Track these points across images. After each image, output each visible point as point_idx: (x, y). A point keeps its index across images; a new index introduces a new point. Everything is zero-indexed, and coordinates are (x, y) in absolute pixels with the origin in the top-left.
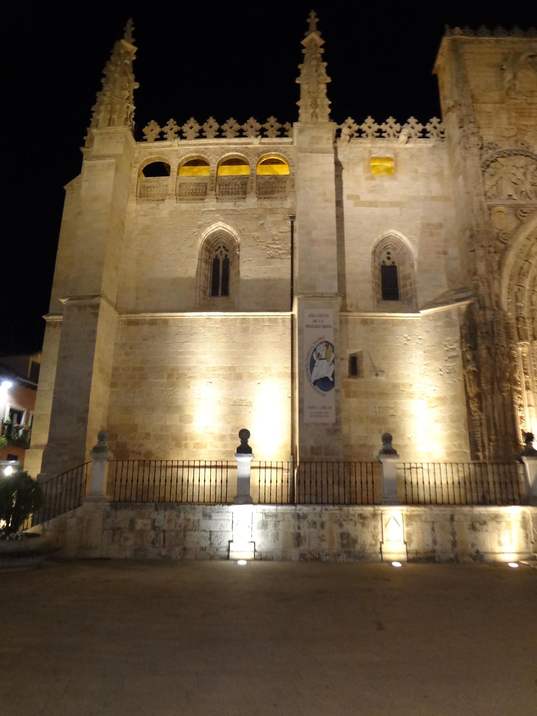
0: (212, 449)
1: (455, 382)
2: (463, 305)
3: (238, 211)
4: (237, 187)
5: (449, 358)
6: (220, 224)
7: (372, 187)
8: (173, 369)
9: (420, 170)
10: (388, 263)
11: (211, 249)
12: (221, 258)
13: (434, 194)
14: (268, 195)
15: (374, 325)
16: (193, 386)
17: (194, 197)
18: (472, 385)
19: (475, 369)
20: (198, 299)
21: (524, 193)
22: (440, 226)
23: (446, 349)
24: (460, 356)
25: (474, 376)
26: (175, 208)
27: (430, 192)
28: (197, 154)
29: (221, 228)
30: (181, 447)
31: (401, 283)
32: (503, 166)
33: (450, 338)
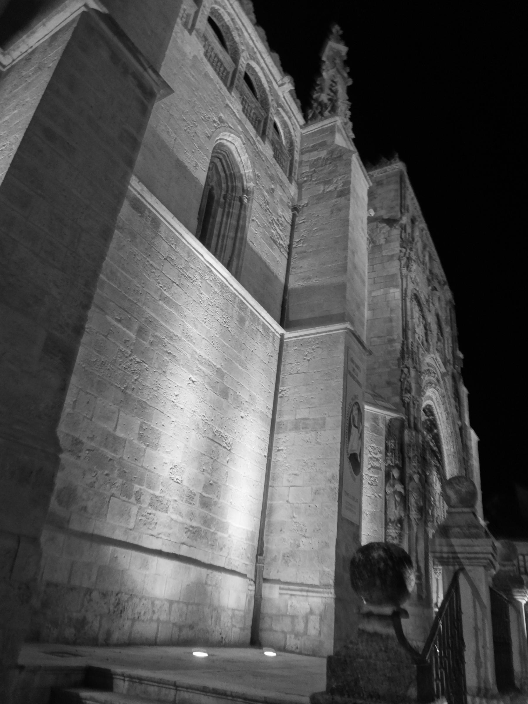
0: (175, 517)
1: (376, 497)
2: (390, 415)
3: (257, 147)
5: (372, 467)
6: (238, 143)
8: (150, 321)
16: (172, 374)
18: (398, 508)
23: (370, 456)
24: (383, 469)
25: (401, 499)
28: (230, 23)
29: (232, 148)
30: (129, 496)
33: (374, 445)
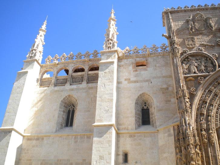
4: (79, 79)
7: (136, 74)
9: (157, 65)
10: (145, 108)
11: (67, 106)
12: (71, 110)
13: (164, 75)
14: (92, 82)
15: (135, 138)
17: (62, 84)
19: (180, 157)
20: (58, 128)
21: (201, 70)
22: (167, 89)
26: (53, 89)
27: (162, 74)
31: (151, 116)
32: (191, 60)
